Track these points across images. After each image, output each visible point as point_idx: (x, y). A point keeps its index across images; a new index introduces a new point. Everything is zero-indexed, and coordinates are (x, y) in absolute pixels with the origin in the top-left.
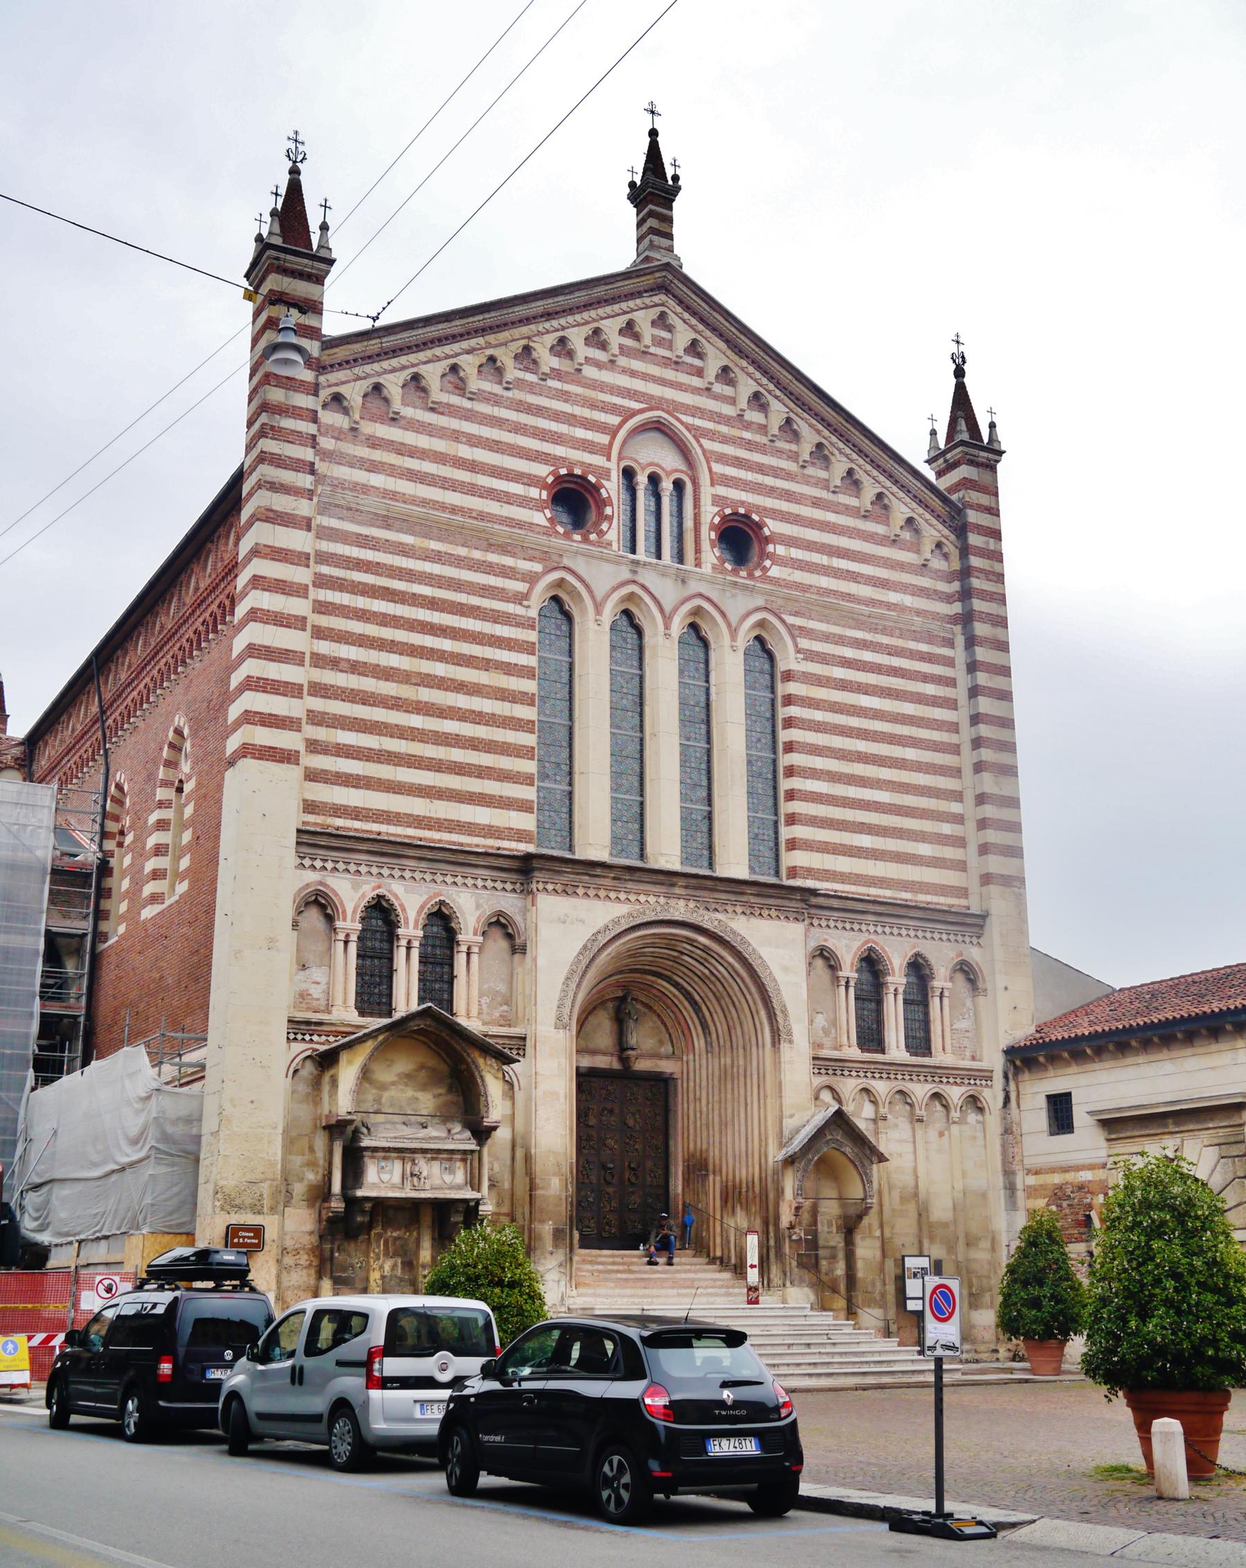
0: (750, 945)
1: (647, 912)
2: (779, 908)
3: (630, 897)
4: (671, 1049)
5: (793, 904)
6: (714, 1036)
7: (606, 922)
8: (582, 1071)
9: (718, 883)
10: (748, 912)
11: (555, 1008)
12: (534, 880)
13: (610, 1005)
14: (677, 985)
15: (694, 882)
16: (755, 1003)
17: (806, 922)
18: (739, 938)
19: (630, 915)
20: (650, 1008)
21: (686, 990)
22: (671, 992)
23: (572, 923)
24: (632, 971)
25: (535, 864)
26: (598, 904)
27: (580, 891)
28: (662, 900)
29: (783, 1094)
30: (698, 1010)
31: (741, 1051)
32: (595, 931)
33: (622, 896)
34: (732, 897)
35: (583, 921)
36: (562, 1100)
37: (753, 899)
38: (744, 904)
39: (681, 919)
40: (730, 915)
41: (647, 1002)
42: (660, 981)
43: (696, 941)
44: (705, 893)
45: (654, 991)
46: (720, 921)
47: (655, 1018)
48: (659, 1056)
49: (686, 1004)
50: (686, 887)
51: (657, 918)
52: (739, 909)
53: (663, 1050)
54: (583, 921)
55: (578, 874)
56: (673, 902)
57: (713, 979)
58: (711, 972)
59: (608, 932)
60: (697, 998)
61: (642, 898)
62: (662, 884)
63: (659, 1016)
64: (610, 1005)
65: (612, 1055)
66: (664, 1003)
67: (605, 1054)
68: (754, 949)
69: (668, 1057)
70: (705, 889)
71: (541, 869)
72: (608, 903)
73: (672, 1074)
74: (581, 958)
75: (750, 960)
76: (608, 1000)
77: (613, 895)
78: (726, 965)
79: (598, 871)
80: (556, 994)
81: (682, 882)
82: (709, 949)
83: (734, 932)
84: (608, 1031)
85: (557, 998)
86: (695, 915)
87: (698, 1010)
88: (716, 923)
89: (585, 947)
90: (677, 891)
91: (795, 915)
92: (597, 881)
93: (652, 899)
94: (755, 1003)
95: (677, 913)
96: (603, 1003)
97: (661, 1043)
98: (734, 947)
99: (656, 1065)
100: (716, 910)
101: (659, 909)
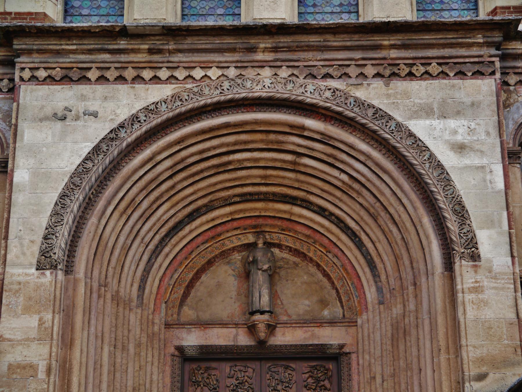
0: (391, 118)
1: (206, 91)
2: (443, 61)
3: (177, 74)
4: (341, 311)
5: (475, 51)
6: (383, 277)
7: (134, 111)
8: (191, 353)
9: (329, 37)
10: (387, 72)
11: (38, 238)
12: (18, 66)
13: (237, 257)
14: (321, 211)
15: (285, 40)
16: (415, 208)
17: (498, 75)
18: (370, 112)
19: (175, 97)
20: (304, 256)
21: (338, 218)
22: (323, 226)
23: (77, 118)
24: (246, 198)
25: (18, 44)
26: (123, 89)
27: (93, 75)
28: (232, 72)
29: (463, 342)
30: (360, 245)
31: (411, 288)
32: (115, 125)
33: (164, 74)
34: (358, 55)
35: (95, 115)
36: (42, 375)
37: (394, 54)
38: (378, 62)
39: (264, 95)
40: (352, 81)
41: (297, 246)
42: (297, 210)
43: (303, 128)
44: (309, 55)
45: (299, 228)
46: (335, 91)
47: (313, 269)
48: (320, 323)
49: (343, 237)
50: (275, 50)
51: (223, 98)
52: (370, 71)
53: (326, 313)
54: (95, 115)
55: (90, 52)
56: (250, 73)
57: (356, 186)
58: (351, 177)
59: (136, 126)
60: (352, 224)
61: (198, 73)
62: (233, 50)
63: (318, 266)
64: (237, 257)
65: (236, 325)
66: (321, 245)
67: (223, 325)
68: (399, 125)
69: (332, 323)
70: (309, 48)
71: (29, 52)
72: (139, 87)
73: (342, 346)
74: (90, 164)
75: (393, 142)
76: (234, 249)
77: (147, 74)
78: (362, 158)
79: (123, 44)
80: (44, 220)
81: (265, 43)
82: (331, 138)
83: (360, 103)
84: (234, 294)
85: (44, 225)
86: (290, 86)
87: (360, 245)
88: (328, 94)
89: (96, 150)
90: (260, 56)
91: (476, 68)
92: (123, 58)
93: (214, 73)
94: (415, 208)
95: (259, 87)
96: (224, 254)
97: (324, 303)
98: (363, 125)
99: (313, 336)
100: (327, 76)
101: (226, 85)
